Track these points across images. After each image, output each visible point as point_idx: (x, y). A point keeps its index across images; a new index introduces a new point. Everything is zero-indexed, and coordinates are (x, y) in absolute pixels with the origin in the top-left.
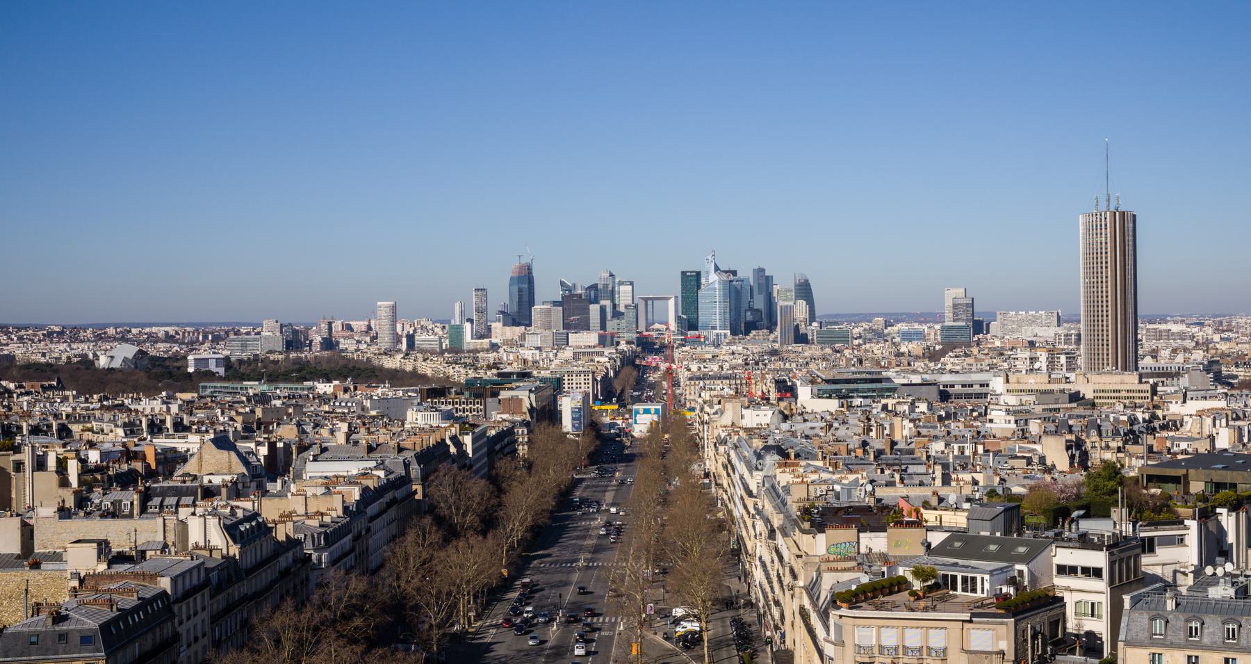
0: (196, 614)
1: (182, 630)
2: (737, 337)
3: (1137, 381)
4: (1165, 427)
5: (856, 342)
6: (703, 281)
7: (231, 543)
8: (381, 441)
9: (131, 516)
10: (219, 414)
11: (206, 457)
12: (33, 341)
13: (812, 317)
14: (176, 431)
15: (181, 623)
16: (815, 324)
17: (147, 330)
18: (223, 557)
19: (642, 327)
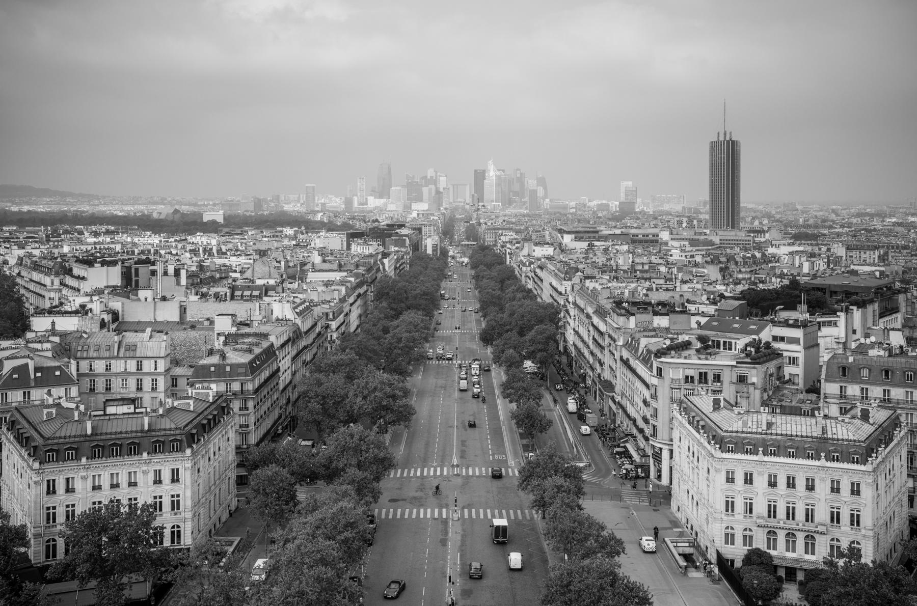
1: (280, 365)
7: (297, 317)
11: (257, 269)
13: (546, 196)
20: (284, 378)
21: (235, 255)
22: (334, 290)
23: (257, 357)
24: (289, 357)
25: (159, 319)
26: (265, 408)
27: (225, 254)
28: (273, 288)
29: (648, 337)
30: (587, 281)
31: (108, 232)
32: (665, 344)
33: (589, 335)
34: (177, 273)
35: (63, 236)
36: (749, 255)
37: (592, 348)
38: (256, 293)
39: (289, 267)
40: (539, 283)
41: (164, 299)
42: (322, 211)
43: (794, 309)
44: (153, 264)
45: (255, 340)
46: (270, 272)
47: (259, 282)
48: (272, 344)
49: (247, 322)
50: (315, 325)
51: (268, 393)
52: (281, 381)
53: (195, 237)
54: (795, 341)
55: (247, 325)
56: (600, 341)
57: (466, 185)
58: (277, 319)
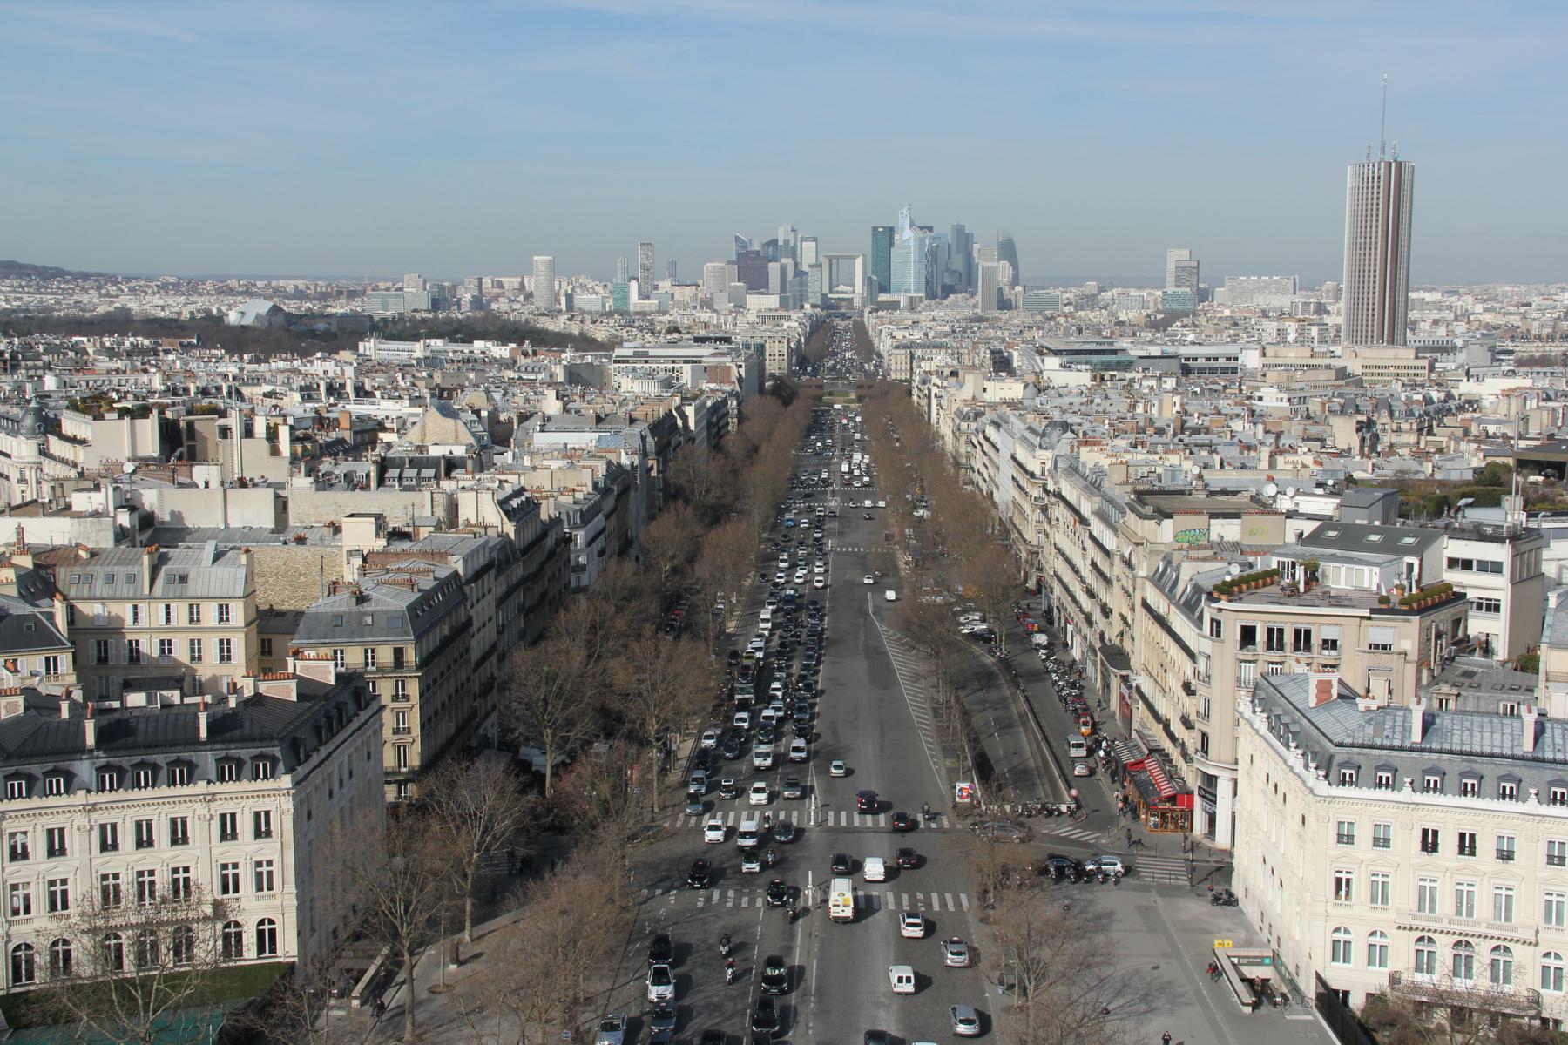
0: (484, 596)
1: (472, 612)
2: (933, 302)
3: (1413, 356)
4: (1461, 408)
5: (1067, 309)
6: (896, 237)
7: (505, 519)
8: (608, 411)
9: (366, 487)
10: (400, 378)
11: (430, 425)
12: (146, 293)
13: (1015, 281)
14: (357, 395)
15: (472, 606)
16: (1019, 288)
17: (274, 283)
18: (499, 536)
19: (826, 290)
20: (478, 643)
22: (584, 467)
23: (427, 597)
25: (235, 523)
26: (442, 696)
27: (369, 394)
29: (1198, 559)
30: (1084, 450)
31: (135, 351)
32: (1229, 573)
34: (272, 434)
35: (45, 358)
36: (1419, 397)
38: (428, 473)
41: (243, 483)
43: (1496, 503)
44: (223, 414)
45: (421, 565)
47: (435, 451)
49: (406, 529)
51: (449, 667)
52: (474, 643)
53: (311, 362)
54: (1496, 568)
56: (1106, 569)
57: (854, 258)
58: (467, 522)
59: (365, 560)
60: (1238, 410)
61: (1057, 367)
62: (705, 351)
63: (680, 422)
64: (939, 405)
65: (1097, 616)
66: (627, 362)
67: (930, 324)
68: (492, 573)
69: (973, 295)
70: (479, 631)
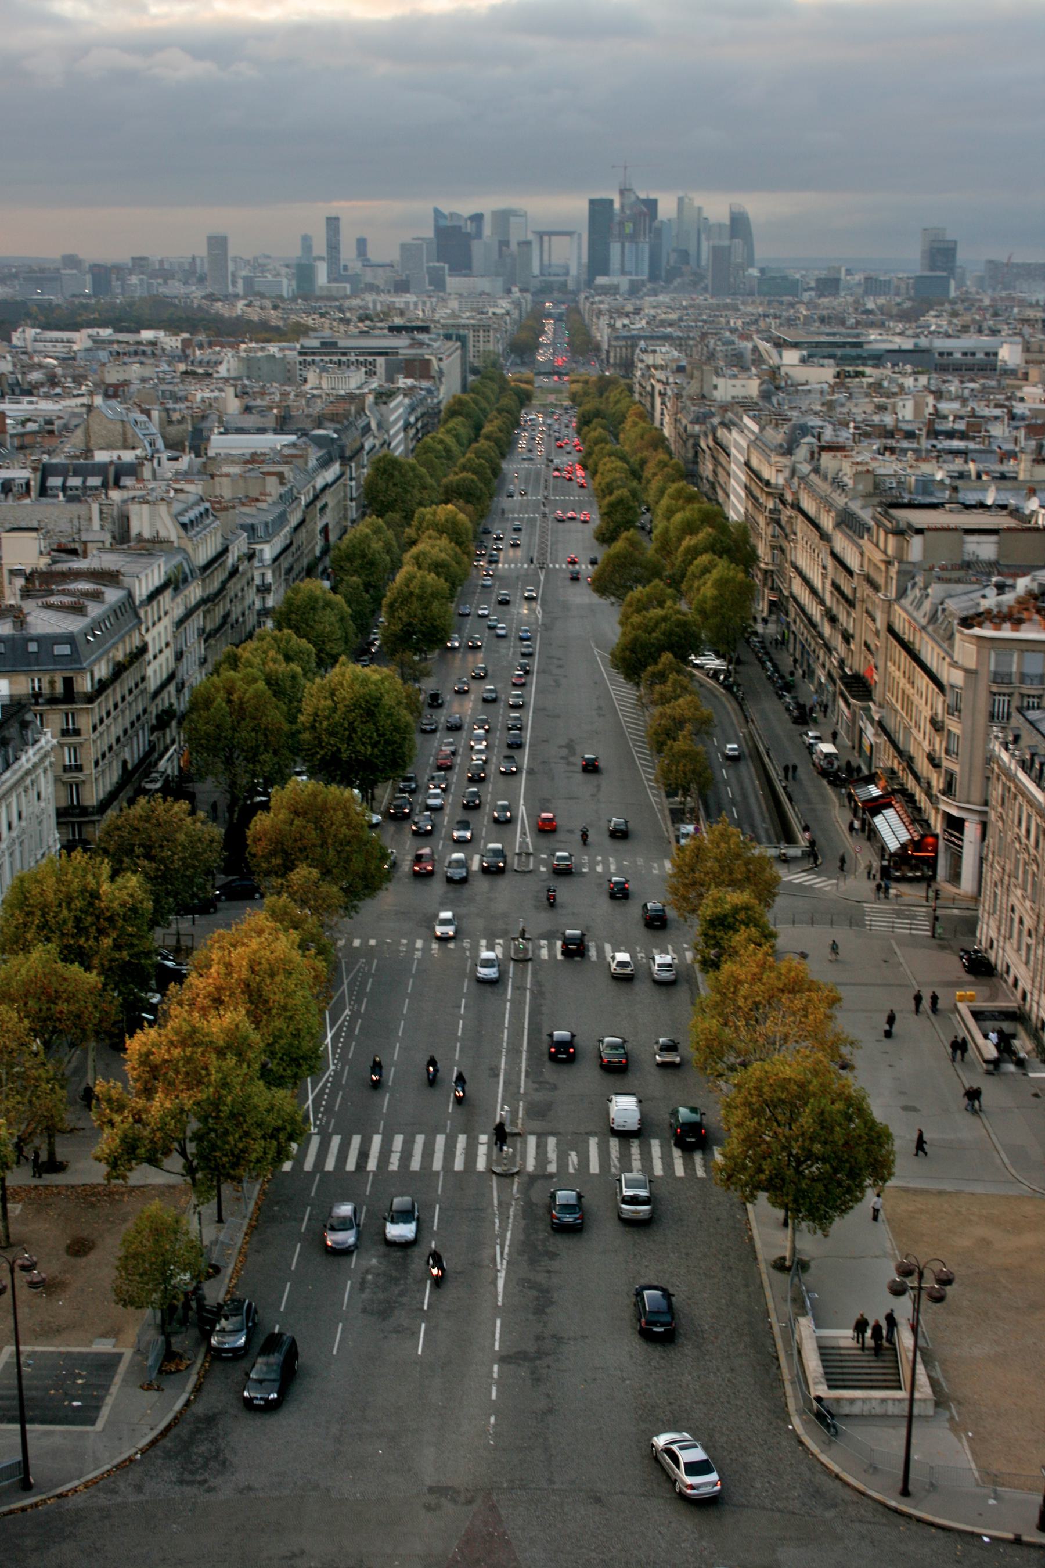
1: (148, 638)
11: (95, 427)
15: (147, 630)
20: (155, 670)
21: (47, 396)
23: (96, 624)
24: (166, 621)
26: (116, 730)
28: (132, 470)
30: (826, 459)
33: (824, 576)
37: (828, 602)
38: (94, 481)
39: (171, 422)
40: (722, 458)
42: (244, 297)
46: (124, 433)
47: (101, 456)
48: (130, 596)
50: (225, 551)
52: (150, 671)
55: (74, 552)
56: (847, 591)
59: (27, 579)
60: (997, 412)
61: (796, 361)
62: (401, 342)
63: (374, 426)
64: (663, 403)
65: (838, 642)
66: (314, 354)
67: (652, 312)
68: (168, 593)
69: (702, 277)
70: (155, 657)
